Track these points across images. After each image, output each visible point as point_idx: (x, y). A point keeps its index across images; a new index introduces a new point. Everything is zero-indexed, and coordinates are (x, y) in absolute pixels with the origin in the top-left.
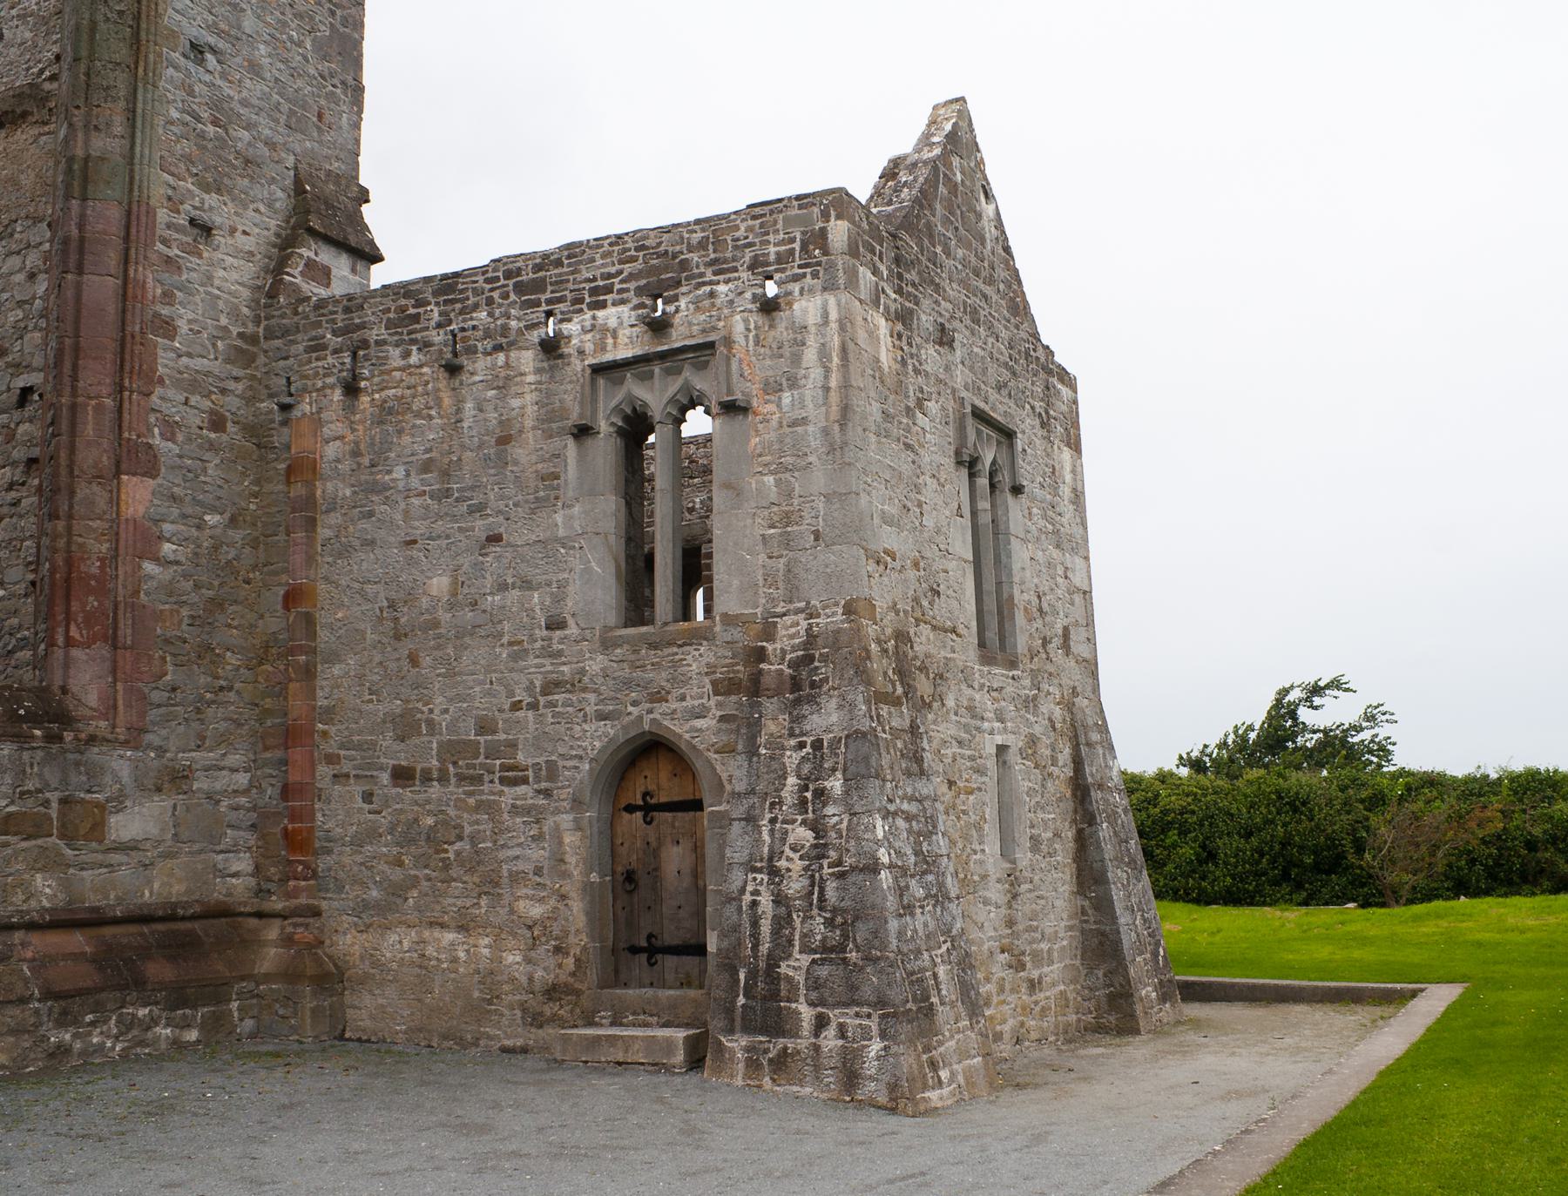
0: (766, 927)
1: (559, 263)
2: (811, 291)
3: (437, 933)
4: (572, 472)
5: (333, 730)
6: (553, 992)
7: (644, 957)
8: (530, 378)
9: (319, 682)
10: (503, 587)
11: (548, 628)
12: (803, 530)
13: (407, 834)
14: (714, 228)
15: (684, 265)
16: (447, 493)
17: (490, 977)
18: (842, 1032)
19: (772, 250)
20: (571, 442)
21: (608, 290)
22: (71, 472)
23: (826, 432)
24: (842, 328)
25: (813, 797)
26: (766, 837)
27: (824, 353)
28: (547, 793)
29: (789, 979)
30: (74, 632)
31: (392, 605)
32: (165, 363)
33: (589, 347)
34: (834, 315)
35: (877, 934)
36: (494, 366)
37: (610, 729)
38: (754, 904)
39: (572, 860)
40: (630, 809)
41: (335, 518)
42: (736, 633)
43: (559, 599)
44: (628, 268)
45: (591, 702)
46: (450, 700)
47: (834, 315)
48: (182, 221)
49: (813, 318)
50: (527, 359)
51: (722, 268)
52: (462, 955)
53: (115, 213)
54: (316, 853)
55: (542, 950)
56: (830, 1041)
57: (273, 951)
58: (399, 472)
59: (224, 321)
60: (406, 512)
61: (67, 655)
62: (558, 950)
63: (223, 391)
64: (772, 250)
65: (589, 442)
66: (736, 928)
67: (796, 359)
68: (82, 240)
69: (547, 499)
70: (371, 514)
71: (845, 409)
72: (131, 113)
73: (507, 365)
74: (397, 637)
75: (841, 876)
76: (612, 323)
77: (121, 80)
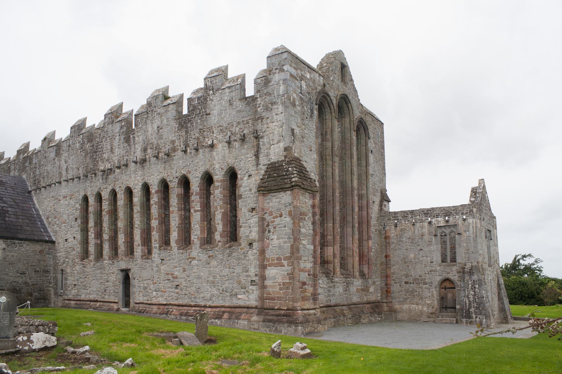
0: (467, 305)
1: (431, 211)
2: (471, 218)
3: (412, 305)
4: (434, 241)
5: (394, 276)
6: (432, 313)
7: (445, 309)
8: (426, 227)
9: (391, 269)
10: (423, 257)
11: (431, 263)
12: (471, 251)
13: (407, 291)
14: (455, 208)
15: (451, 213)
16: (413, 243)
17: (422, 312)
18: (479, 318)
19: (465, 212)
20: (434, 238)
21: (439, 215)
22: (362, 240)
23: (473, 238)
24: (476, 224)
25: (473, 288)
26: (467, 293)
27: (473, 227)
28: (431, 286)
29: (471, 312)
30: (364, 263)
31: (404, 258)
33: (436, 223)
34: (474, 222)
35: (484, 306)
36: (420, 225)
37: (441, 277)
38: (465, 302)
39: (435, 295)
40: (442, 288)
41: (393, 245)
42: (460, 265)
43: (432, 259)
44: (442, 212)
45: (438, 274)
46: (414, 272)
47: (474, 222)
49: (471, 222)
50: (426, 224)
51: (457, 214)
52: (417, 308)
53: (366, 202)
54: (391, 294)
55: (430, 308)
56: (478, 320)
57: (386, 308)
58: (405, 239)
60: (406, 245)
61: (363, 266)
62: (433, 308)
64: (465, 212)
65: (436, 237)
66: (463, 305)
67: (469, 228)
68: (362, 206)
69: (430, 244)
70: (400, 245)
71: (476, 235)
72: (367, 186)
73: (422, 225)
74: (405, 263)
75: (478, 298)
76: (440, 220)
77: (365, 182)
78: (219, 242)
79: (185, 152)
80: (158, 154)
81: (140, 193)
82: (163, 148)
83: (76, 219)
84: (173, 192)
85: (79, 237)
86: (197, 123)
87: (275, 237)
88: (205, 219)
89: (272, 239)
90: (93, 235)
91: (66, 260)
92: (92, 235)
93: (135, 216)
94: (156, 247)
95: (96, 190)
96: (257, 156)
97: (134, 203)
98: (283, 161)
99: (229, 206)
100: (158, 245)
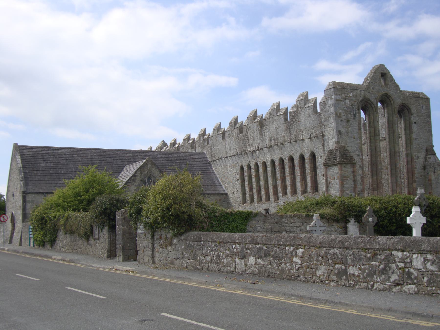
32: (416, 172)
48: (416, 157)
59: (421, 166)
63: (422, 173)
70: (437, 185)
72: (411, 148)
78: (310, 192)
79: (290, 142)
80: (277, 143)
81: (270, 165)
82: (279, 140)
83: (238, 180)
84: (286, 165)
85: (240, 190)
86: (294, 126)
87: (333, 190)
88: (303, 180)
89: (332, 191)
90: (248, 190)
91: (235, 205)
92: (247, 190)
93: (269, 178)
94: (280, 196)
95: (247, 163)
96: (323, 146)
97: (268, 171)
98: (335, 149)
99: (313, 173)
100: (281, 195)
